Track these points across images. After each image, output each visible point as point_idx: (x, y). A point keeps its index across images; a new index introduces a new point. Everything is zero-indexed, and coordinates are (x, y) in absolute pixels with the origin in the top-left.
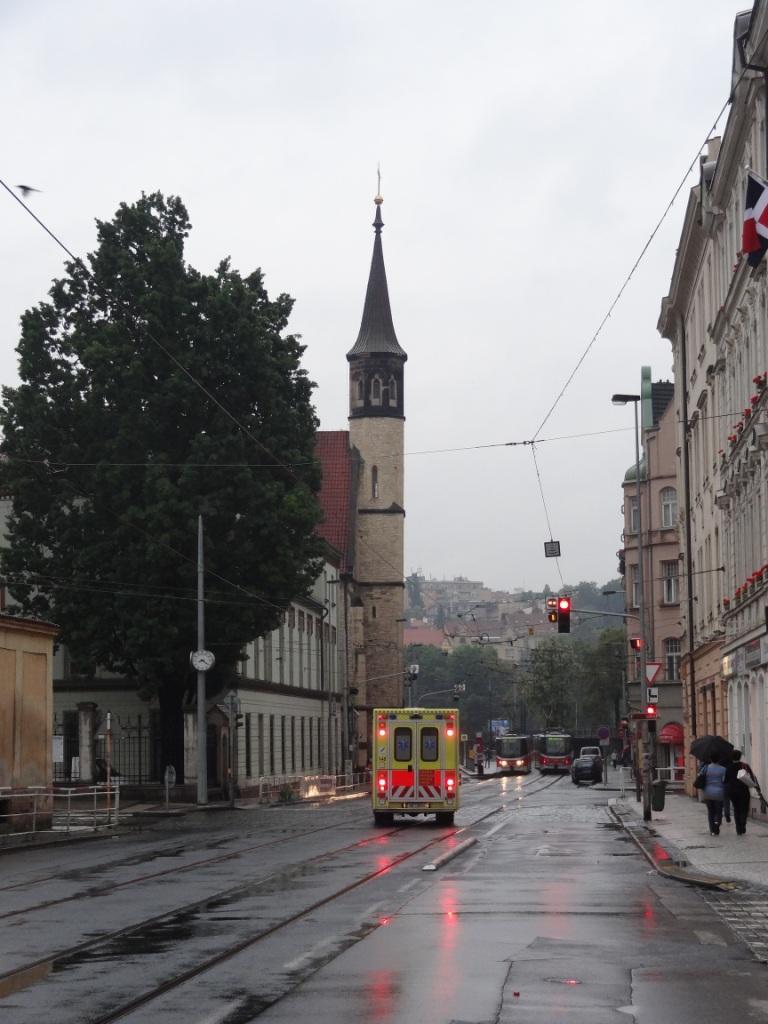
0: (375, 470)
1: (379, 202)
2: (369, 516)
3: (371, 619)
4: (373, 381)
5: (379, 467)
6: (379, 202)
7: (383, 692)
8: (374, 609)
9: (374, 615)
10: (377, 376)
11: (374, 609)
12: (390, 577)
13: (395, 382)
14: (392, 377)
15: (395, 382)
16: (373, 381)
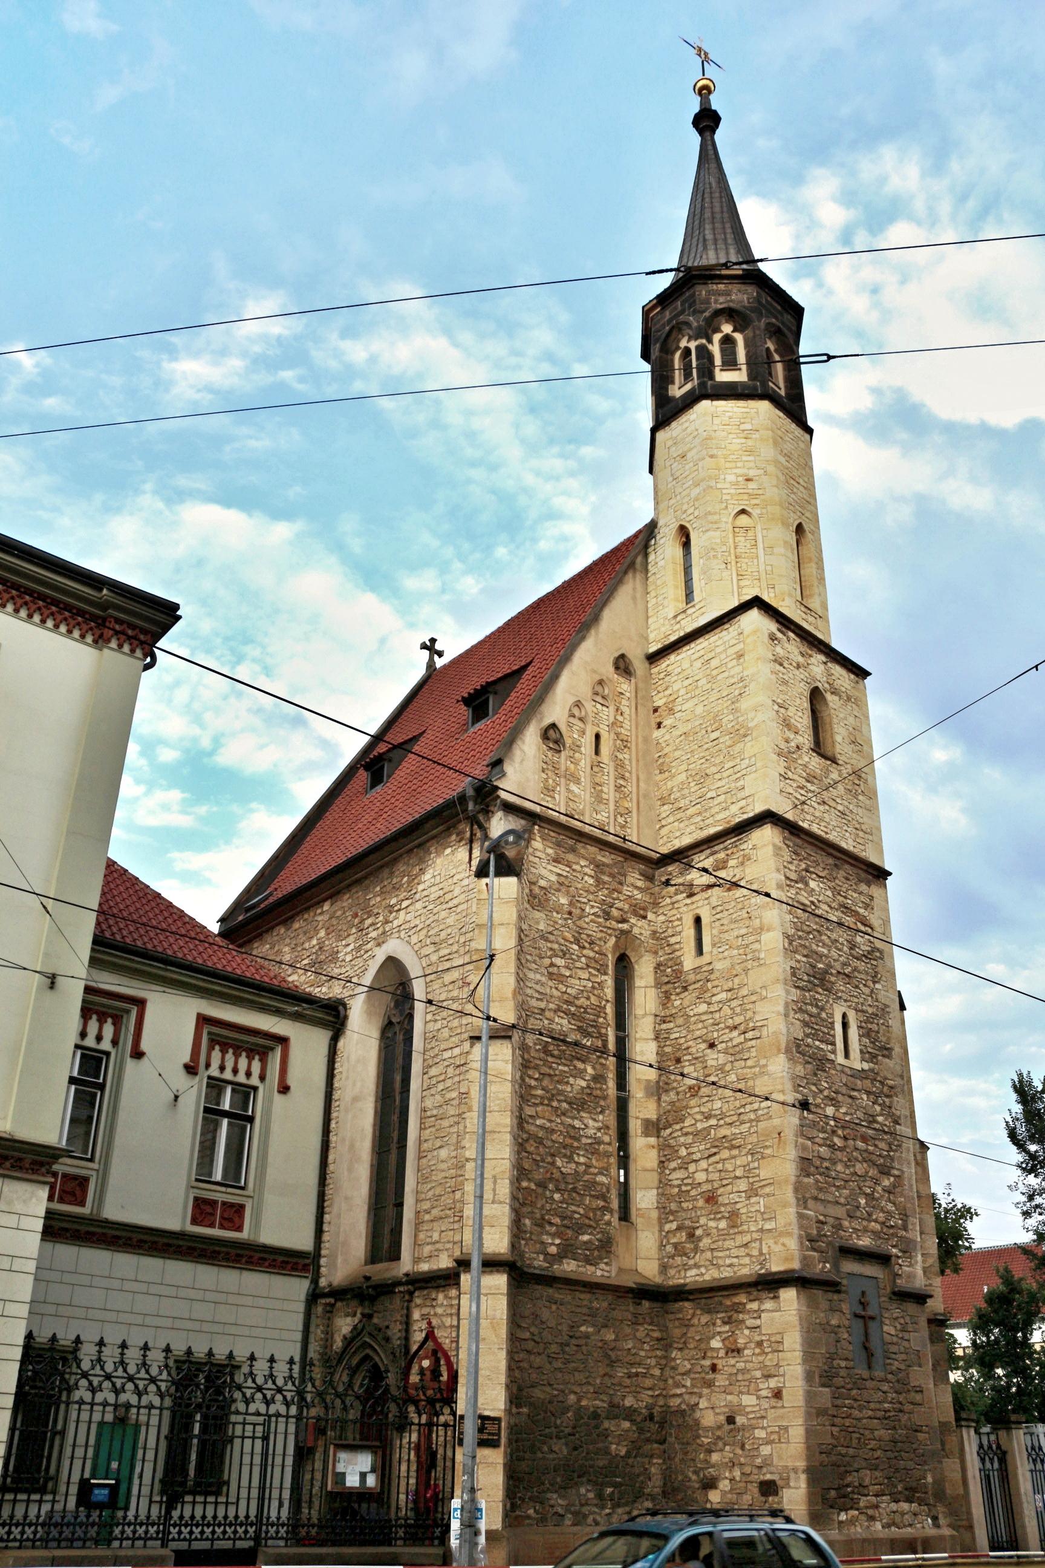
0: (684, 535)
1: (704, 92)
2: (673, 657)
3: (689, 961)
4: (678, 355)
5: (688, 525)
6: (704, 92)
7: (733, 1217)
8: (698, 920)
9: (700, 951)
10: (683, 343)
11: (698, 920)
12: (734, 809)
13: (739, 337)
14: (727, 328)
15: (739, 337)
16: (678, 355)
